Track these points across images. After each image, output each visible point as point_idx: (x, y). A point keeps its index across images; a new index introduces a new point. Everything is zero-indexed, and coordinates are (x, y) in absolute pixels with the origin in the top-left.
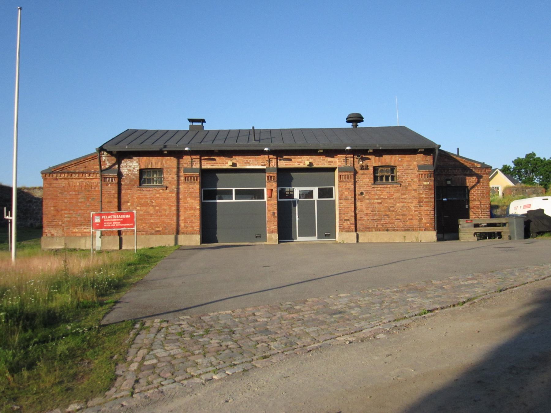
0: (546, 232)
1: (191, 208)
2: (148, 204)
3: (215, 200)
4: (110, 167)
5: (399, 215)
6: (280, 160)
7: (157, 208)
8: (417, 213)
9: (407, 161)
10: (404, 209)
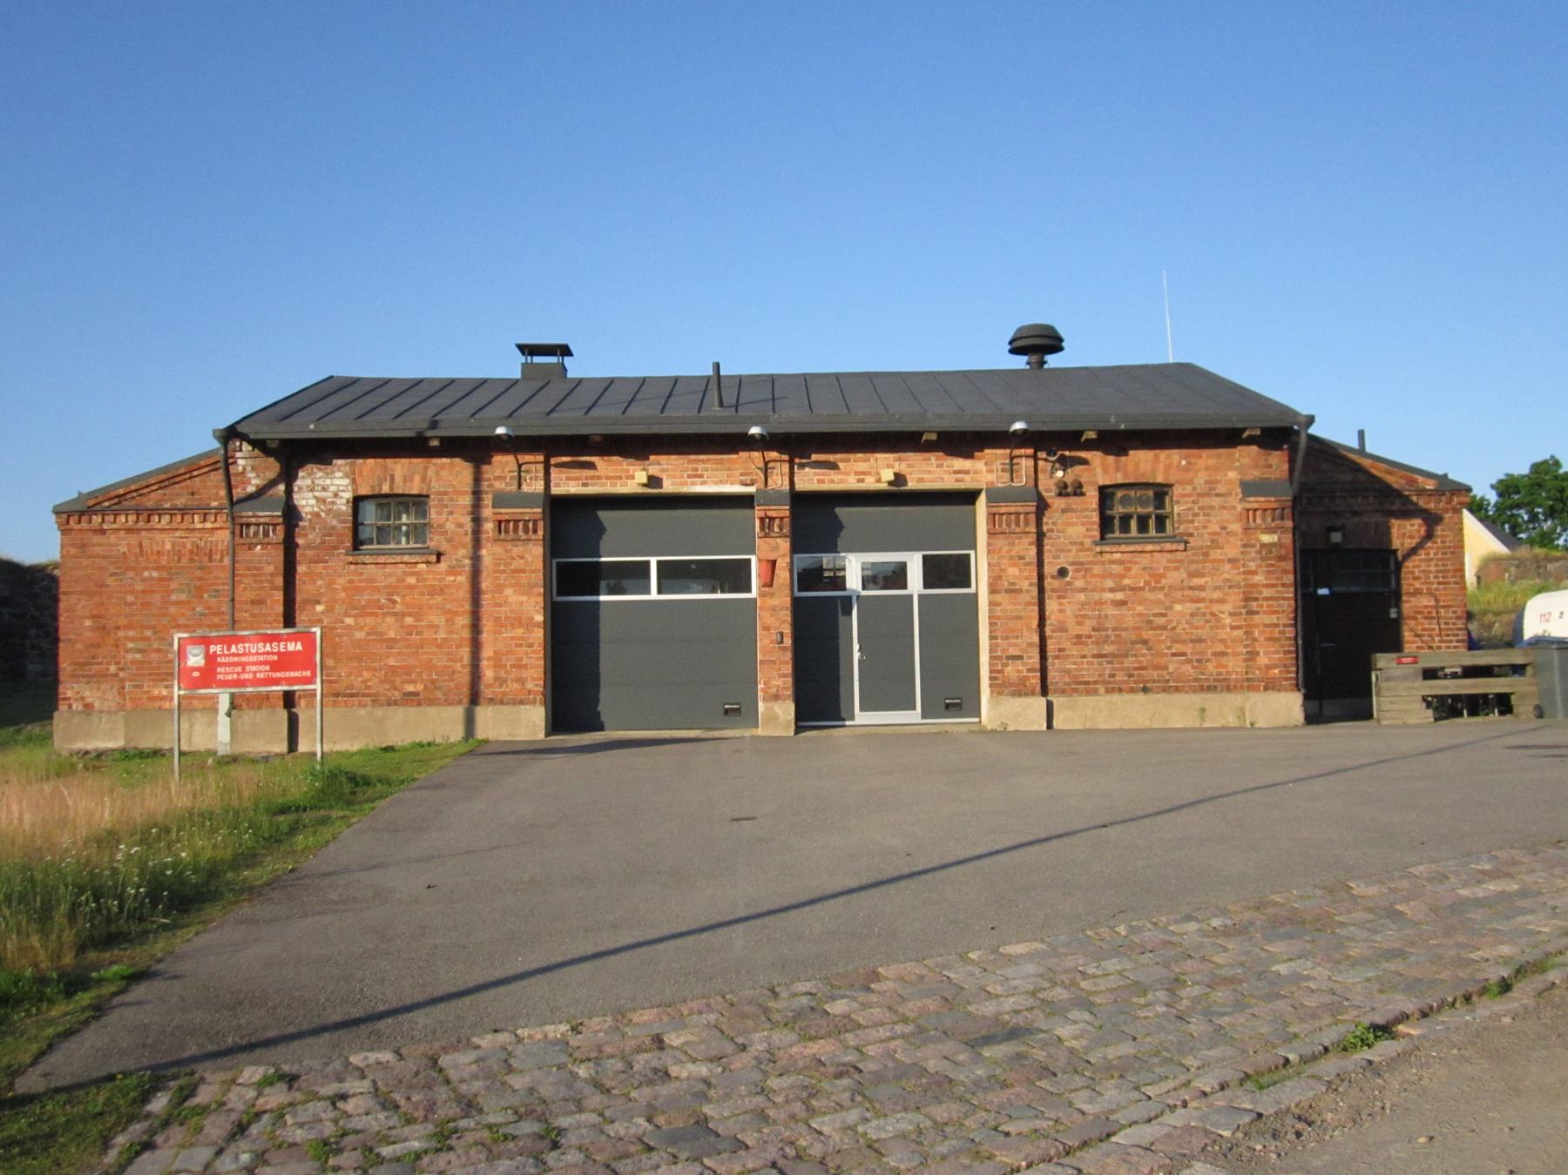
1: (520, 621)
2: (381, 608)
3: (598, 594)
4: (261, 491)
5: (1183, 642)
6: (802, 466)
7: (409, 620)
8: (1239, 633)
9: (1207, 468)
10: (1198, 621)
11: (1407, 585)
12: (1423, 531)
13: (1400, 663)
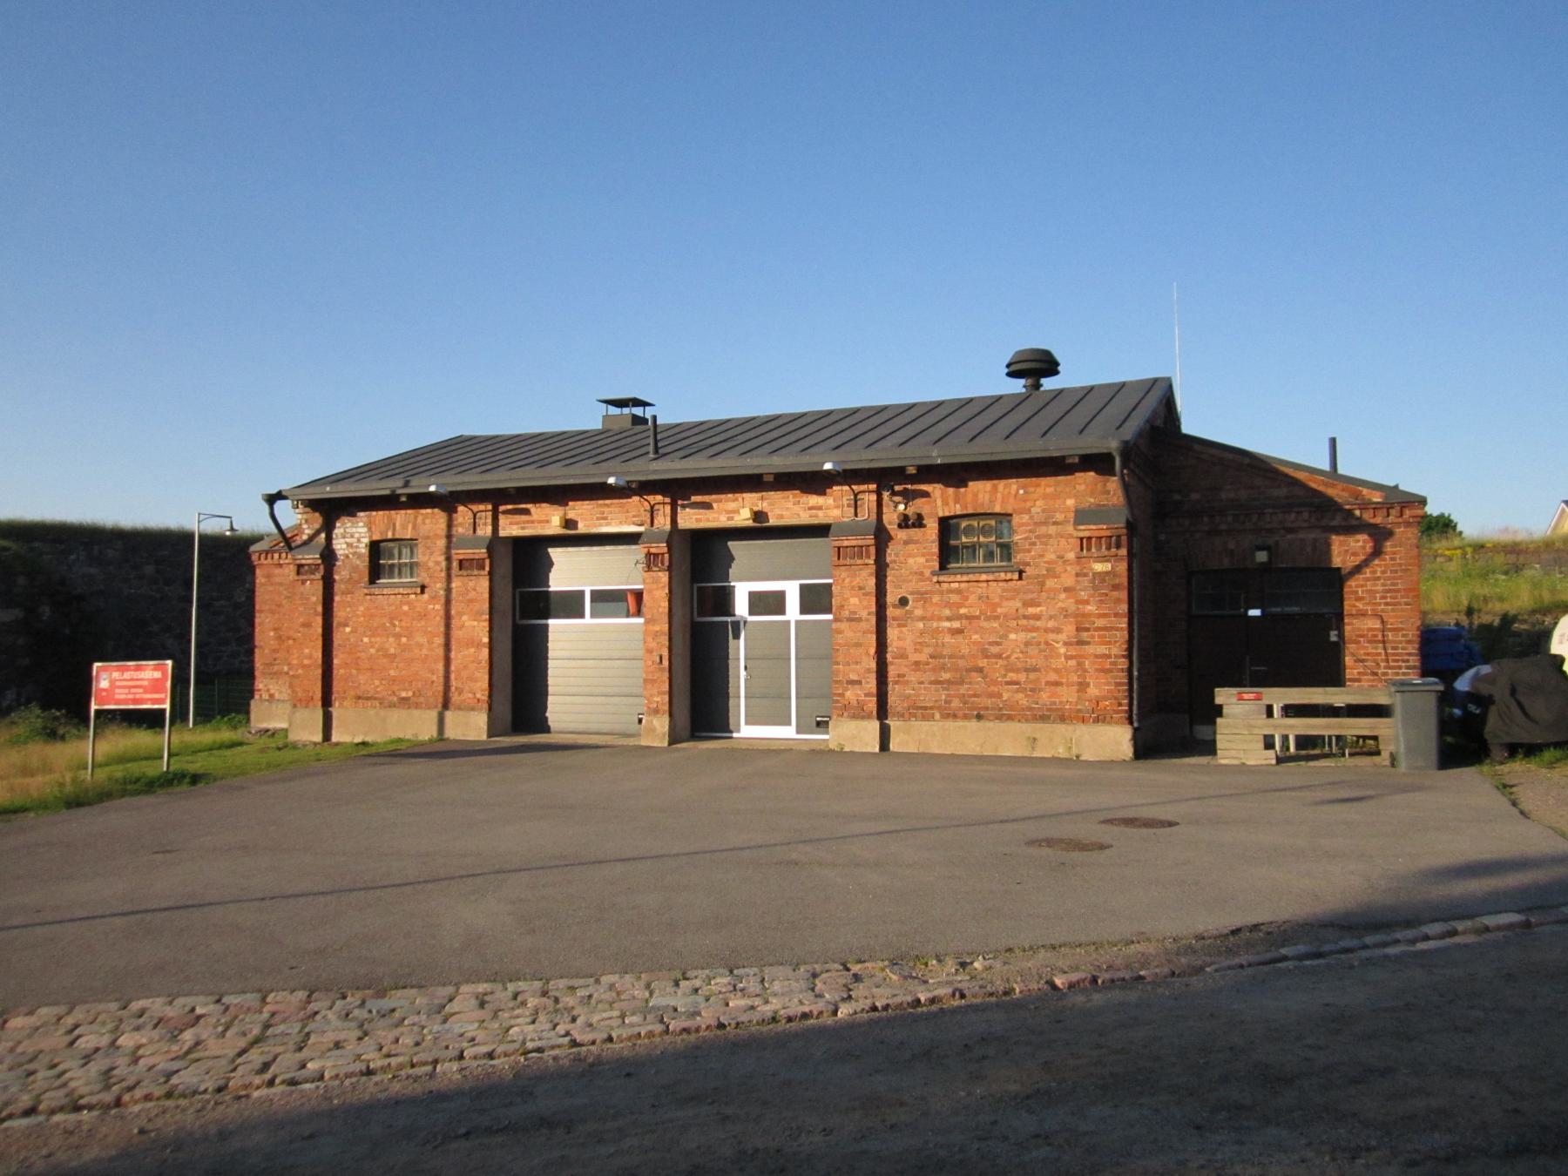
0: (1547, 746)
4: (312, 538)
5: (1017, 671)
6: (684, 507)
8: (1072, 663)
9: (1045, 497)
10: (1033, 651)
11: (1349, 605)
12: (1369, 547)
13: (1241, 699)
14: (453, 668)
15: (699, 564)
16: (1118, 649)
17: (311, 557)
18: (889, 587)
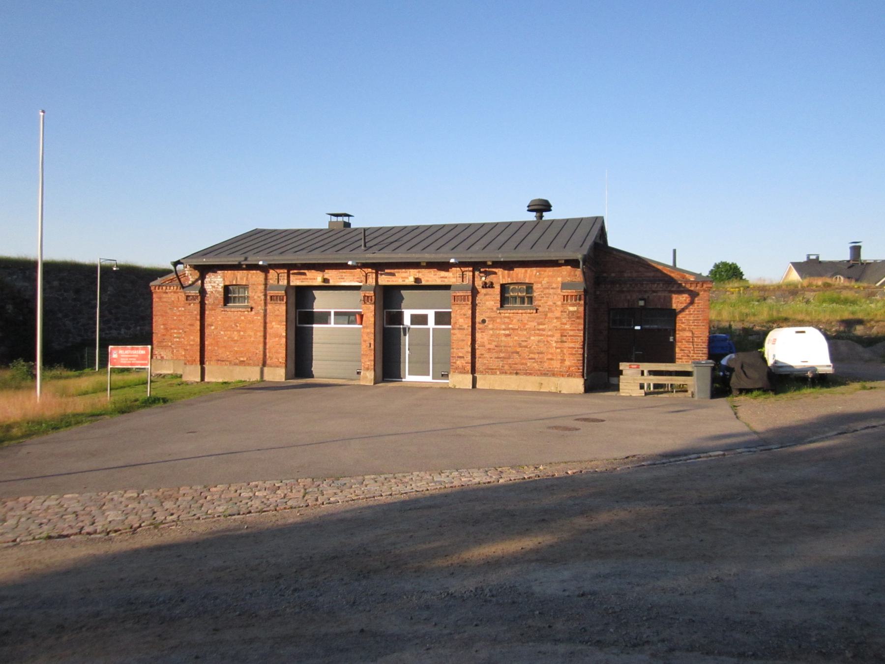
4: (194, 283)
5: (534, 353)
8: (559, 350)
9: (548, 276)
10: (541, 345)
11: (679, 326)
12: (688, 300)
14: (267, 347)
15: (388, 300)
16: (579, 345)
17: (194, 292)
18: (477, 314)
